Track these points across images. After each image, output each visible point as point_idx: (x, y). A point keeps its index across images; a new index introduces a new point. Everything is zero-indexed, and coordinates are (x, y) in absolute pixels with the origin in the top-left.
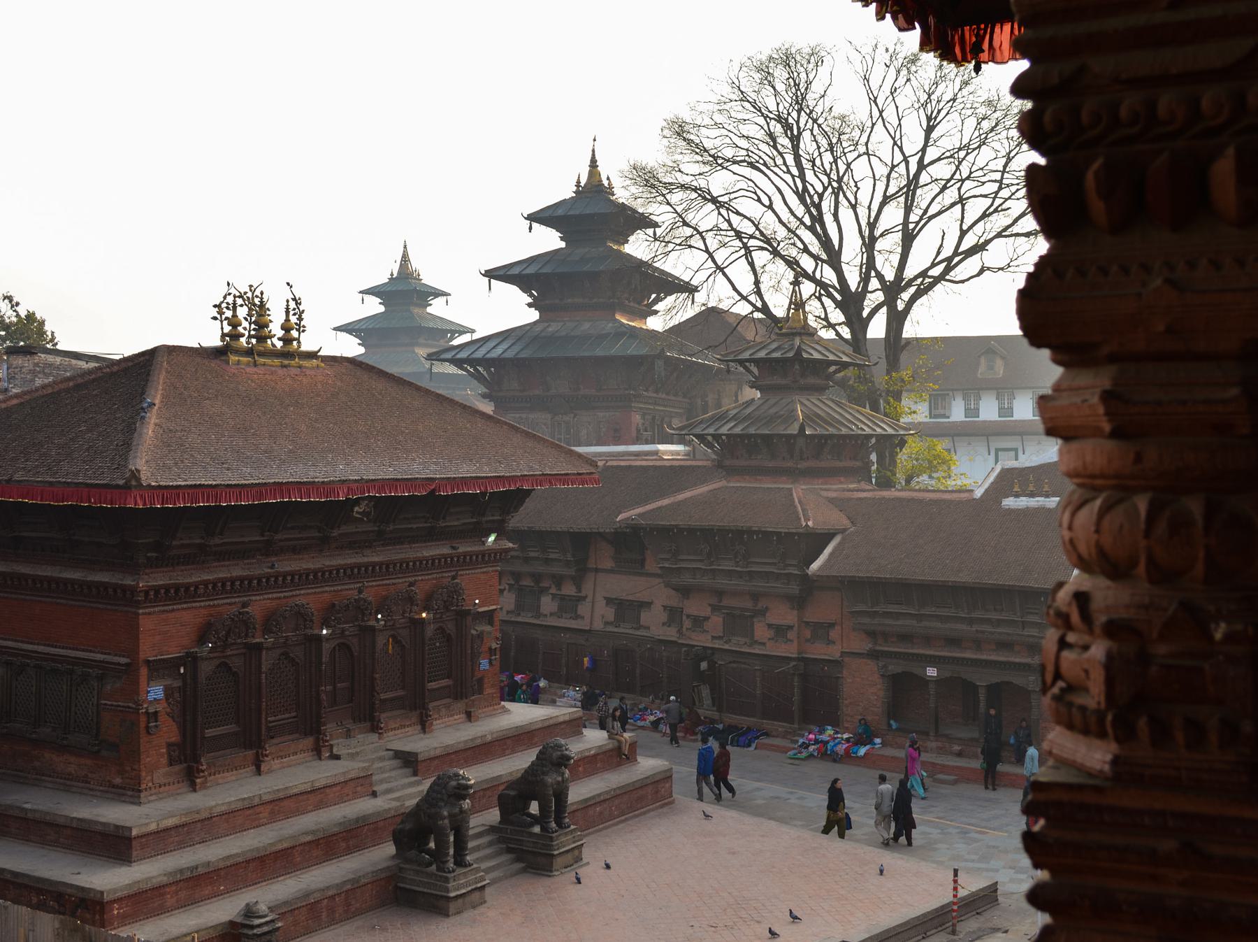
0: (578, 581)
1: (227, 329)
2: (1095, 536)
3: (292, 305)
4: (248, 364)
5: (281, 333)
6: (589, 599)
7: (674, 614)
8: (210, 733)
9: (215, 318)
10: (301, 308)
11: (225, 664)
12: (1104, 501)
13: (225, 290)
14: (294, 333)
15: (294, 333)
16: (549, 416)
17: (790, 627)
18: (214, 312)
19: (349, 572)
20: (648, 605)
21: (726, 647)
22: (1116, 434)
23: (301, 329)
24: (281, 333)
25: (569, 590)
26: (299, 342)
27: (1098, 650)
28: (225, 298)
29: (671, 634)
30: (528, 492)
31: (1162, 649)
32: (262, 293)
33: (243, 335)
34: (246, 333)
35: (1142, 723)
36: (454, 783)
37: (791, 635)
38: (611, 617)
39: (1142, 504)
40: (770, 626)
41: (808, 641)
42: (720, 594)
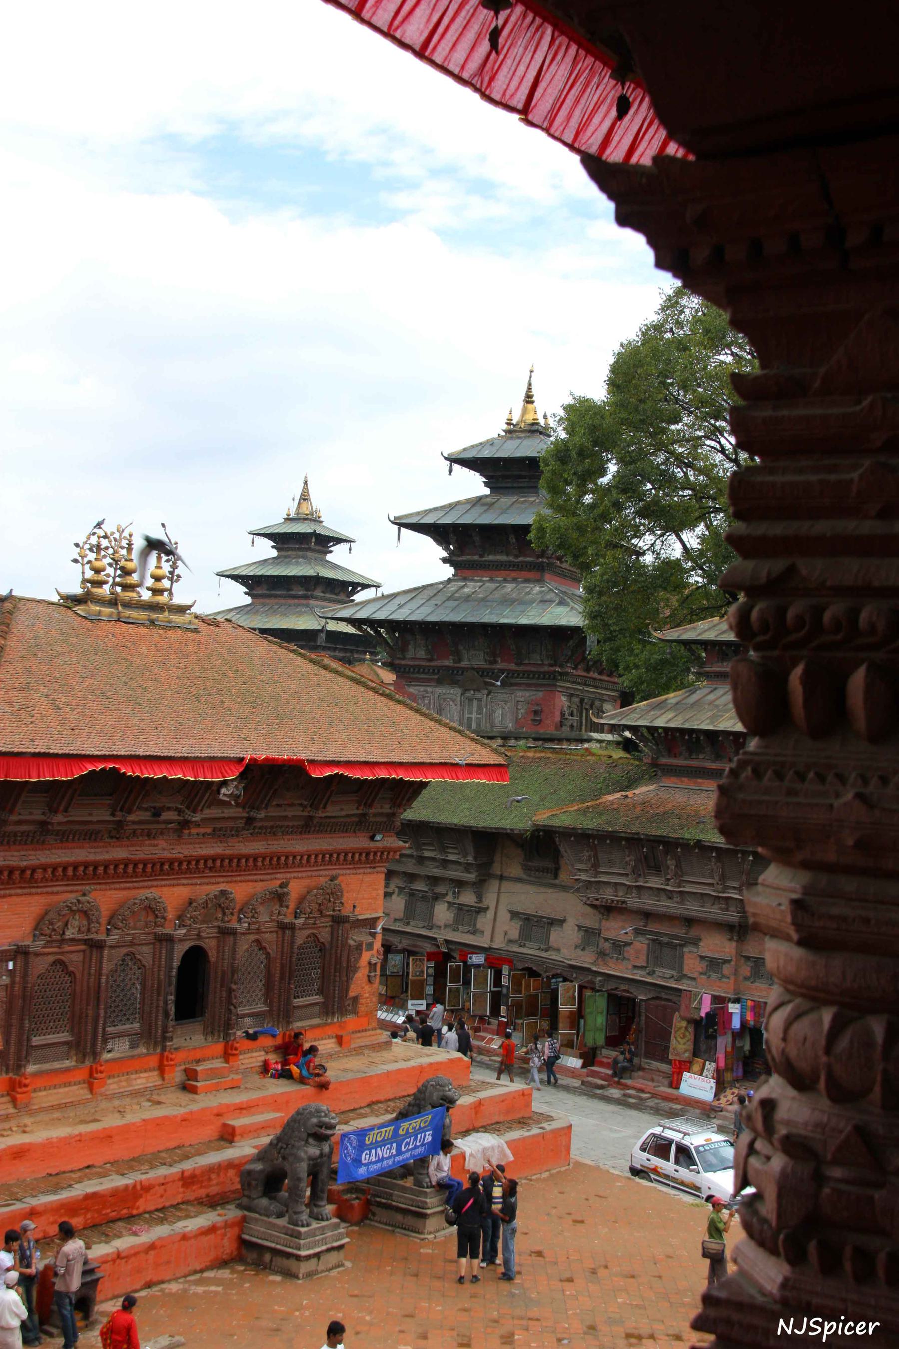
0: (479, 886)
1: (89, 574)
2: (782, 1045)
5: (150, 582)
6: (490, 914)
7: (590, 935)
8: (36, 1041)
9: (76, 561)
11: (61, 962)
12: (792, 1010)
14: (166, 583)
15: (166, 583)
16: (459, 691)
17: (728, 961)
18: (75, 553)
19: (210, 863)
20: (561, 922)
21: (649, 980)
22: (800, 943)
23: (174, 577)
25: (468, 898)
26: (171, 593)
27: (778, 1162)
28: (89, 538)
29: (586, 959)
30: (423, 785)
31: (837, 1172)
32: (131, 535)
33: (106, 582)
34: (111, 580)
35: (812, 1247)
36: (314, 1120)
37: (727, 969)
38: (515, 934)
39: (827, 1016)
40: (702, 958)
41: (746, 979)
42: (648, 915)
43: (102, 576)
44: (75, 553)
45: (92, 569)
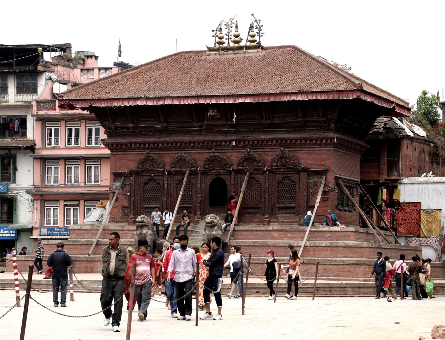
3: (255, 24)
4: (216, 54)
9: (213, 36)
10: (260, 25)
14: (257, 38)
32: (237, 21)
33: (224, 43)
43: (224, 40)
44: (213, 34)
45: (218, 38)
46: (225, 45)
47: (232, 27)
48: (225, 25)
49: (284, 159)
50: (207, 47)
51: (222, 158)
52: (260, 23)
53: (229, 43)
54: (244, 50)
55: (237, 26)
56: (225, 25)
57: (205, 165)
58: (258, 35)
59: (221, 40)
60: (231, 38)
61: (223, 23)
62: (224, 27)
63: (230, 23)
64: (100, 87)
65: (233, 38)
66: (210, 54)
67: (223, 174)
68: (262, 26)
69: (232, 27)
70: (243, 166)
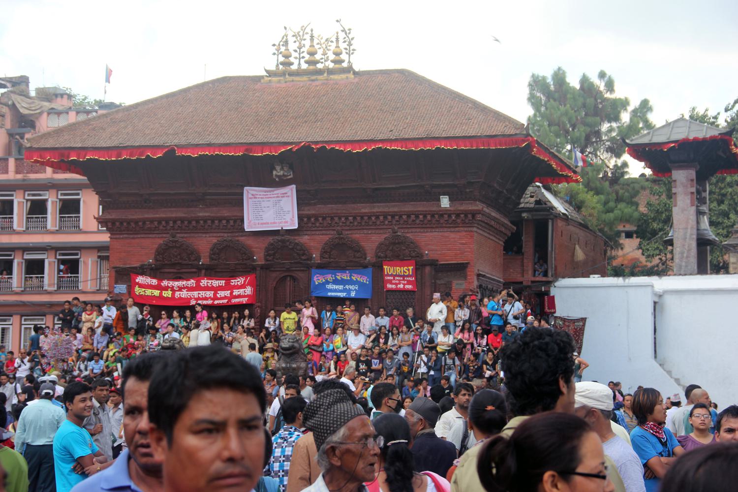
3: (342, 35)
4: (279, 82)
9: (274, 54)
10: (351, 36)
13: (283, 32)
14: (344, 56)
24: (332, 57)
32: (312, 30)
43: (292, 59)
44: (274, 50)
45: (283, 56)
46: (294, 67)
47: (305, 40)
48: (293, 36)
49: (397, 246)
50: (266, 71)
51: (297, 244)
52: (349, 33)
53: (299, 64)
54: (325, 75)
55: (312, 37)
56: (293, 36)
57: (267, 255)
58: (347, 53)
59: (287, 60)
60: (303, 57)
61: (290, 34)
62: (291, 40)
63: (301, 34)
64: (94, 129)
65: (307, 57)
66: (270, 80)
67: (296, 270)
68: (353, 39)
69: (305, 40)
70: (330, 258)
